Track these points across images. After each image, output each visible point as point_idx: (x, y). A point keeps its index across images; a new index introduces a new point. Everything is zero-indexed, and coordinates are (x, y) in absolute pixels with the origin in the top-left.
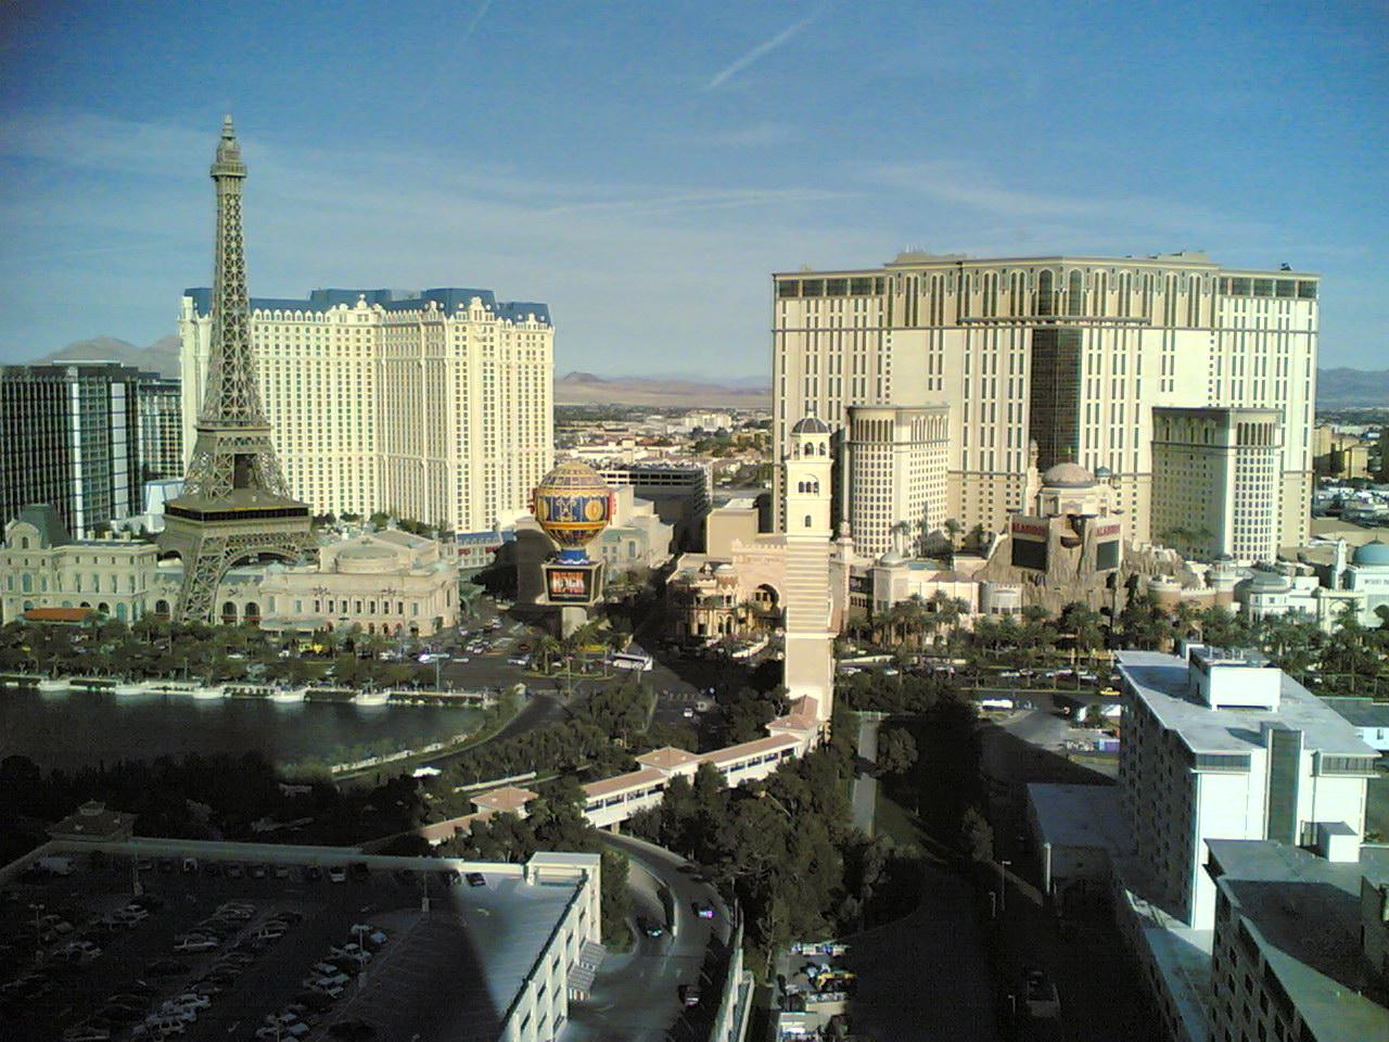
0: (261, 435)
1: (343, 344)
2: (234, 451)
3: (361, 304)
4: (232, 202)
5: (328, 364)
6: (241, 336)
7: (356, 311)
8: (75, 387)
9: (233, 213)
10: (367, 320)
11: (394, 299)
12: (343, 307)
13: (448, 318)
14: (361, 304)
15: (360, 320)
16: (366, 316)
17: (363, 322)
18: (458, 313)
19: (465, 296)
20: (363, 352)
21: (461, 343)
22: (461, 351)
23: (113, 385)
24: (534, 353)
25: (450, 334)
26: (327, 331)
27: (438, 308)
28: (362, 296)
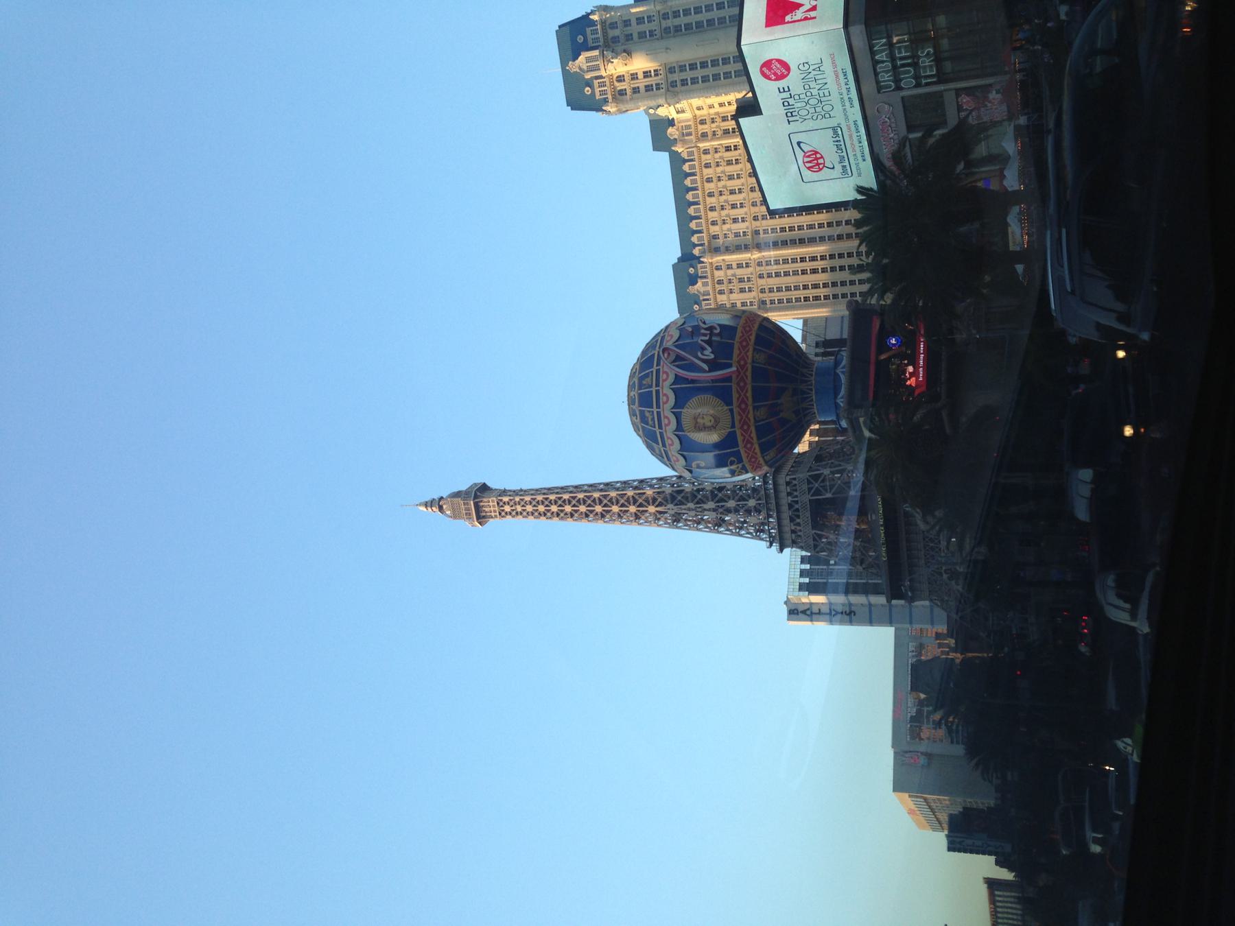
2: (807, 530)
4: (507, 508)
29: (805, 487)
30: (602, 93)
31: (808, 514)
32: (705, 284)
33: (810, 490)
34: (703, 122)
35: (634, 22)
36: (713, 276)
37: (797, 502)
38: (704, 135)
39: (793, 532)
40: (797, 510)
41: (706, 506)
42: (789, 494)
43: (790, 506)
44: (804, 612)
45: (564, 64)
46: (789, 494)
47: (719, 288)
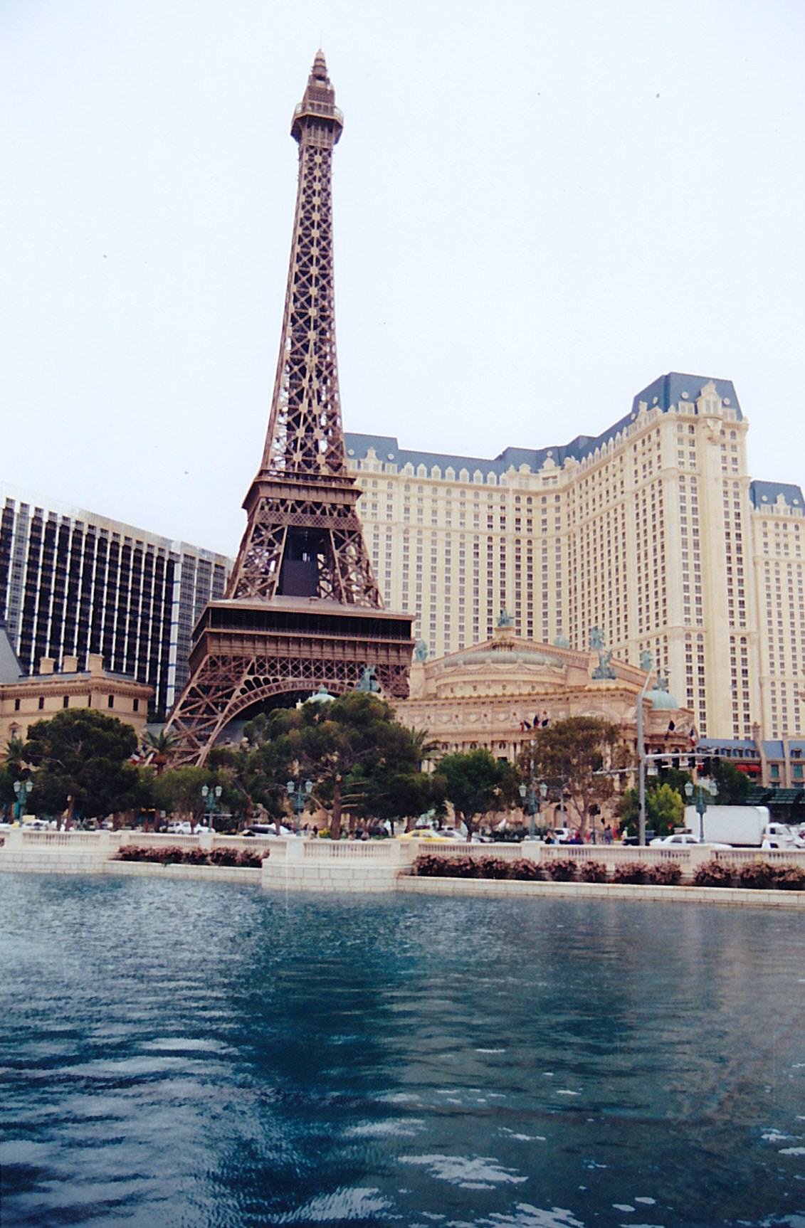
0: (340, 500)
1: (524, 516)
2: (288, 520)
3: (549, 463)
4: (318, 159)
5: (503, 540)
6: (318, 350)
7: (542, 474)
8: (178, 569)
9: (317, 173)
10: (555, 483)
12: (525, 469)
13: (666, 410)
14: (549, 463)
17: (551, 486)
18: (681, 404)
20: (551, 525)
21: (687, 449)
22: (687, 460)
24: (786, 546)
25: (670, 433)
26: (503, 498)
28: (550, 453)
29: (345, 527)
30: (683, 408)
31: (309, 524)
32: (376, 467)
33: (342, 532)
34: (529, 500)
35: (735, 455)
36: (383, 478)
37: (323, 513)
38: (518, 499)
40: (313, 512)
41: (315, 402)
42: (334, 506)
43: (318, 505)
45: (715, 380)
46: (334, 506)
47: (370, 481)
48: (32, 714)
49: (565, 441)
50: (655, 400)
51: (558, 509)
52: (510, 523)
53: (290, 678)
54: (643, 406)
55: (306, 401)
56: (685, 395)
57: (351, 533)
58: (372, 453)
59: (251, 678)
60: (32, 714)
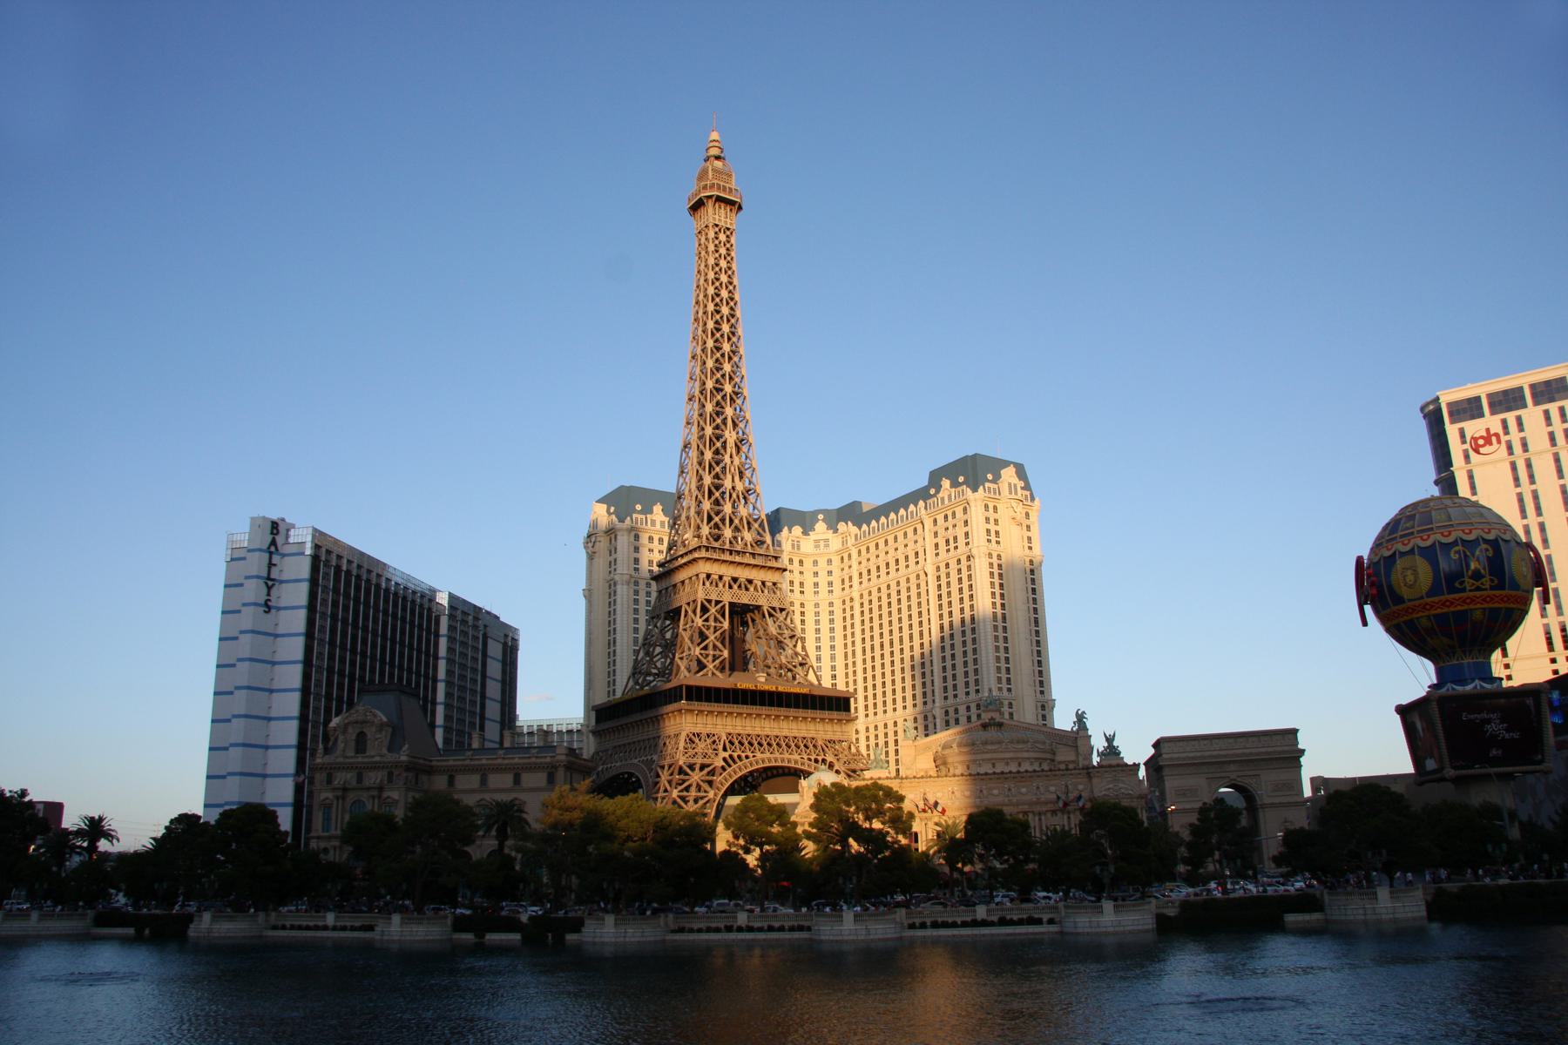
0: (770, 577)
2: (727, 598)
3: (821, 526)
4: (722, 237)
6: (735, 425)
7: (813, 536)
8: (444, 622)
9: (723, 251)
11: (865, 509)
12: (797, 530)
13: (975, 490)
14: (821, 526)
15: (817, 547)
16: (827, 540)
19: (997, 465)
20: (823, 588)
23: (490, 642)
25: (977, 514)
27: (955, 484)
28: (821, 517)
29: (777, 605)
31: (745, 601)
34: (801, 562)
39: (721, 577)
41: (737, 478)
43: (750, 582)
44: (274, 543)
48: (473, 791)
49: (836, 504)
50: (961, 479)
51: (830, 573)
52: (823, 588)
53: (759, 755)
54: (946, 483)
55: (729, 477)
56: (990, 477)
57: (782, 610)
58: (658, 508)
59: (726, 755)
60: (473, 791)
